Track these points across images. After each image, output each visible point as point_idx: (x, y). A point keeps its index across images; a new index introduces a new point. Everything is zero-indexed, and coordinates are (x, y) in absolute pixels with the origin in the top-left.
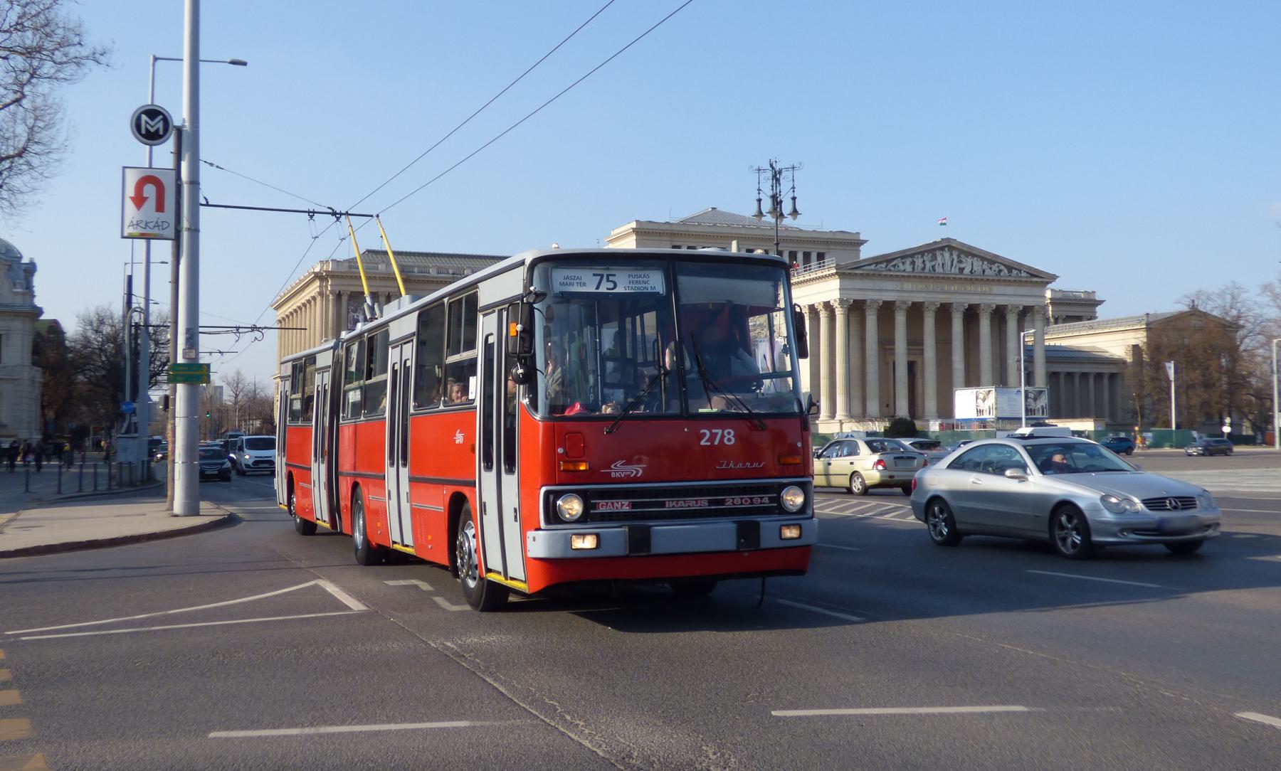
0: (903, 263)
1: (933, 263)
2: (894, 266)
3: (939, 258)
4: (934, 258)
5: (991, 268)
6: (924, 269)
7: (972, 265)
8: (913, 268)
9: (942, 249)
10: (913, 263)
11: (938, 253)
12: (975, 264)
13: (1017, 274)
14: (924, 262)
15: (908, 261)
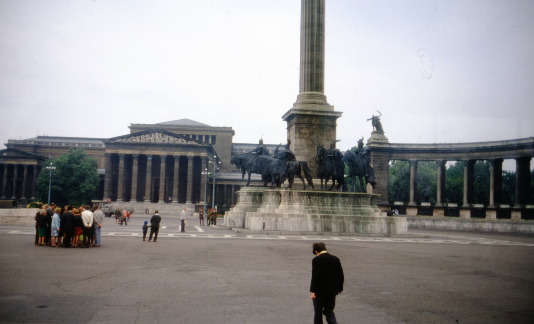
0: (136, 138)
1: (150, 138)
2: (131, 140)
3: (153, 135)
4: (151, 136)
5: (178, 140)
6: (145, 141)
7: (169, 139)
8: (140, 141)
9: (154, 132)
10: (140, 138)
11: (152, 134)
12: (170, 138)
13: (191, 143)
14: (145, 138)
15: (138, 137)
